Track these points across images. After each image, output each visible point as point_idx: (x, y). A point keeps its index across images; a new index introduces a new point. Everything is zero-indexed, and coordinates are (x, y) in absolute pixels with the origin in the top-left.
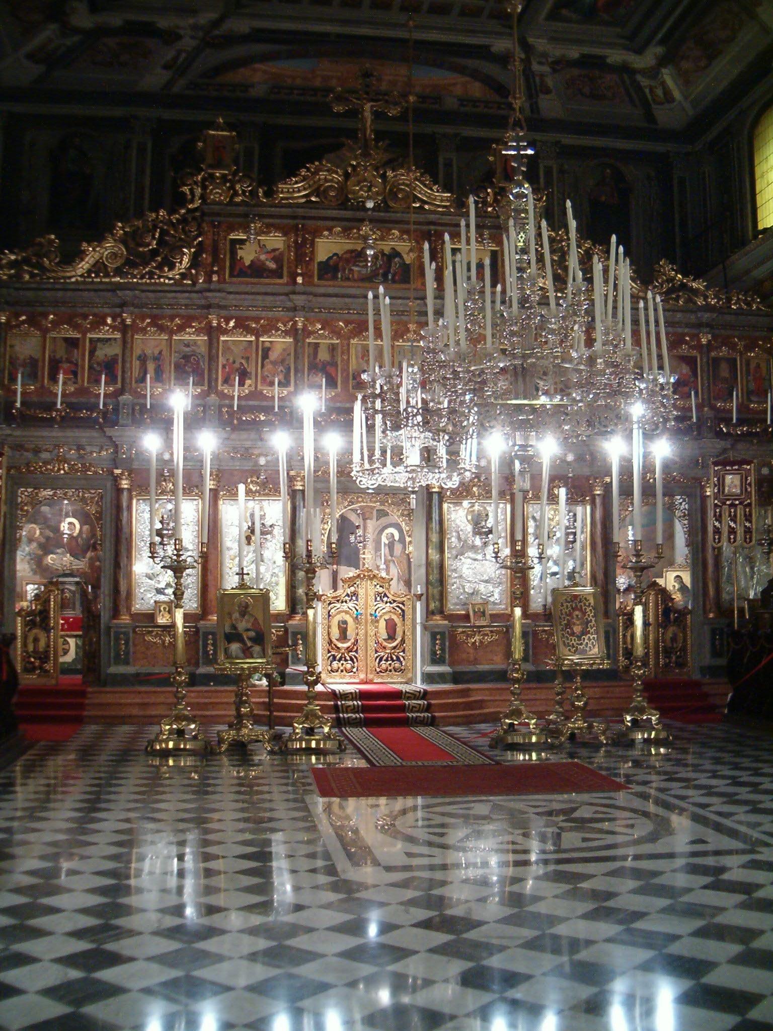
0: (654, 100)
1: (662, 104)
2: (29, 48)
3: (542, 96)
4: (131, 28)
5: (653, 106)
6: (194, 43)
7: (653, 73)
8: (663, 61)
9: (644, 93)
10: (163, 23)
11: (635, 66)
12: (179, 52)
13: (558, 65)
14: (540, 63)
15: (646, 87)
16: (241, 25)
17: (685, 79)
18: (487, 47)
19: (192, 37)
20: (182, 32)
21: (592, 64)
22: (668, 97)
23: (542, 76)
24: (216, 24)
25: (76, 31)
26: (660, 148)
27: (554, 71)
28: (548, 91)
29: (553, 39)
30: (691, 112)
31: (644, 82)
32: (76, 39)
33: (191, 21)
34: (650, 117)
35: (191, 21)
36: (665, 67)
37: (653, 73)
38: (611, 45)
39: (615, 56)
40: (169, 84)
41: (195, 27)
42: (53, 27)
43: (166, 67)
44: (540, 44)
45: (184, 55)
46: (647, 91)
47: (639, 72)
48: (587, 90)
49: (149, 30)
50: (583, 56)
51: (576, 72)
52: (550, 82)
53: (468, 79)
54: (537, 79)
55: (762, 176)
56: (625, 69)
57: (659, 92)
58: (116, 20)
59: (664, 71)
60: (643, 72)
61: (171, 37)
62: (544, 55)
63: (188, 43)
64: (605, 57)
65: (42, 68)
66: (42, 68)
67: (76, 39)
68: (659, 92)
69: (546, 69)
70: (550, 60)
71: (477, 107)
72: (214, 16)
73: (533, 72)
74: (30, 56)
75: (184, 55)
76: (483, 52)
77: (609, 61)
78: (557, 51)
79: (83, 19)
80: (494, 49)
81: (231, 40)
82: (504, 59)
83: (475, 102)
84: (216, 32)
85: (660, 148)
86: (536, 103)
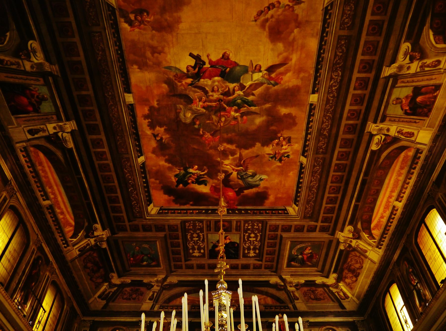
0: (341, 298)
1: (345, 299)
2: (99, 293)
3: (296, 301)
4: (134, 283)
5: (342, 301)
6: (159, 288)
7: (336, 286)
8: (339, 280)
9: (335, 295)
10: (145, 281)
11: (328, 284)
12: (154, 292)
13: (298, 286)
14: (291, 286)
15: (335, 292)
16: (174, 279)
17: (350, 286)
18: (268, 282)
19: (157, 286)
20: (153, 284)
21: (310, 284)
22: (347, 297)
23: (292, 292)
24: (165, 279)
25: (115, 285)
26: (350, 319)
27: (297, 289)
28: (298, 299)
29: (292, 275)
30: (358, 302)
31: (334, 290)
32: (115, 288)
33: (155, 279)
34: (342, 307)
35: (155, 279)
36: (340, 283)
37: (336, 286)
38: (316, 276)
39: (319, 280)
40: (153, 307)
41: (157, 281)
42: (106, 284)
43: (150, 299)
44: (288, 278)
45: (155, 294)
46: (336, 294)
47: (330, 286)
48: (312, 296)
49: (141, 283)
50: (306, 281)
51: (305, 289)
52: (297, 295)
53: (265, 296)
54: (292, 294)
55: (393, 322)
56: (324, 285)
57: (341, 294)
58: (128, 280)
59: (340, 284)
60: (331, 286)
61: (149, 286)
62: (291, 283)
63: (156, 288)
64: (315, 281)
65: (104, 302)
66: (104, 302)
67: (115, 288)
68: (341, 294)
69: (293, 289)
70: (294, 284)
71: (272, 309)
72: (163, 276)
73: (289, 291)
74: (99, 297)
75: (155, 294)
76: (267, 284)
77: (317, 282)
78: (295, 280)
79: (116, 281)
80: (271, 282)
81: (172, 286)
82: (276, 286)
83: (271, 307)
84: (165, 283)
85: (350, 319)
86: (294, 304)
